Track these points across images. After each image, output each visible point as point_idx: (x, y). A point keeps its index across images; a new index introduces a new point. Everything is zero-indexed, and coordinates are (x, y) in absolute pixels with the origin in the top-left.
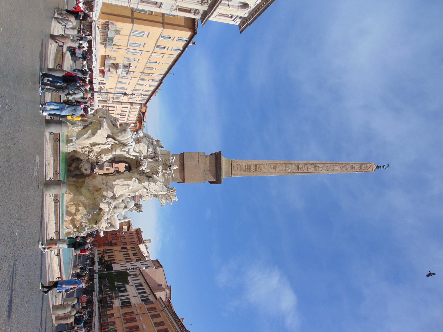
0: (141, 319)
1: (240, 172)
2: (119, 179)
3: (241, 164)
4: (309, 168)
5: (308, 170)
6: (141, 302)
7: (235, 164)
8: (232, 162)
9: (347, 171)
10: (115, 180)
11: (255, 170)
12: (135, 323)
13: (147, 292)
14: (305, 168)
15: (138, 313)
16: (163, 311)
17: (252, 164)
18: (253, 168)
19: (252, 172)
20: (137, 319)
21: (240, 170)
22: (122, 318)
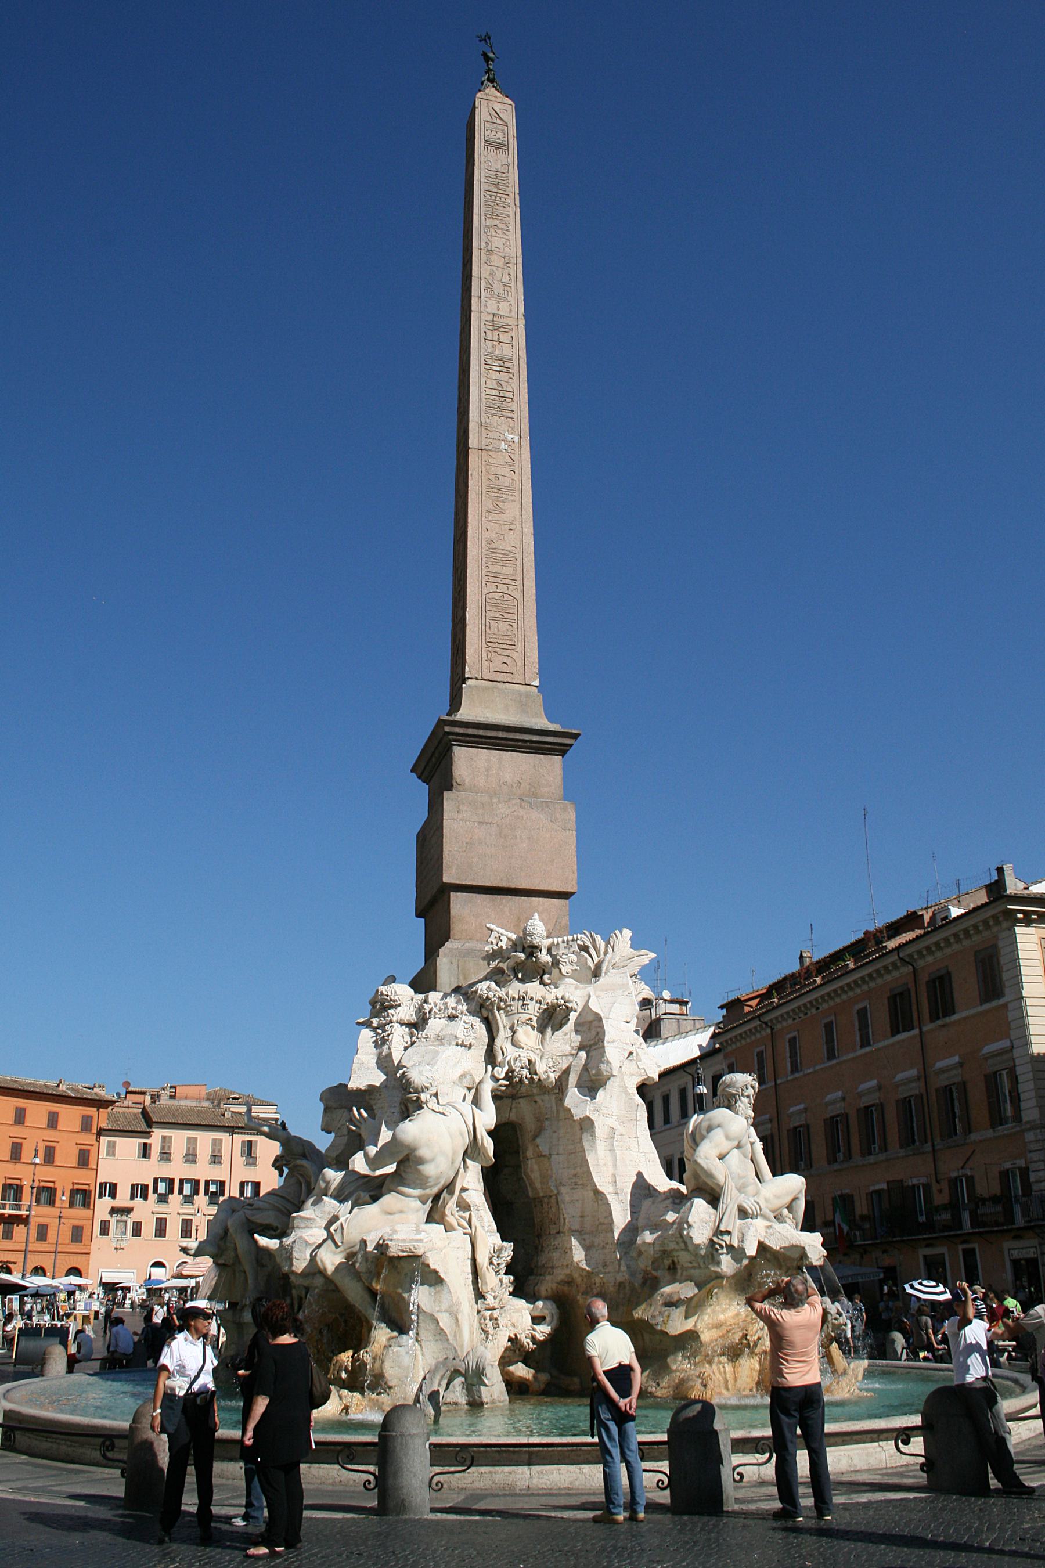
0: (802, 1106)
1: (520, 649)
3: (483, 640)
5: (510, 360)
7: (485, 664)
8: (477, 679)
9: (512, 204)
10: (597, 1193)
13: (683, 1086)
14: (498, 369)
16: (772, 1029)
17: (485, 591)
20: (797, 1124)
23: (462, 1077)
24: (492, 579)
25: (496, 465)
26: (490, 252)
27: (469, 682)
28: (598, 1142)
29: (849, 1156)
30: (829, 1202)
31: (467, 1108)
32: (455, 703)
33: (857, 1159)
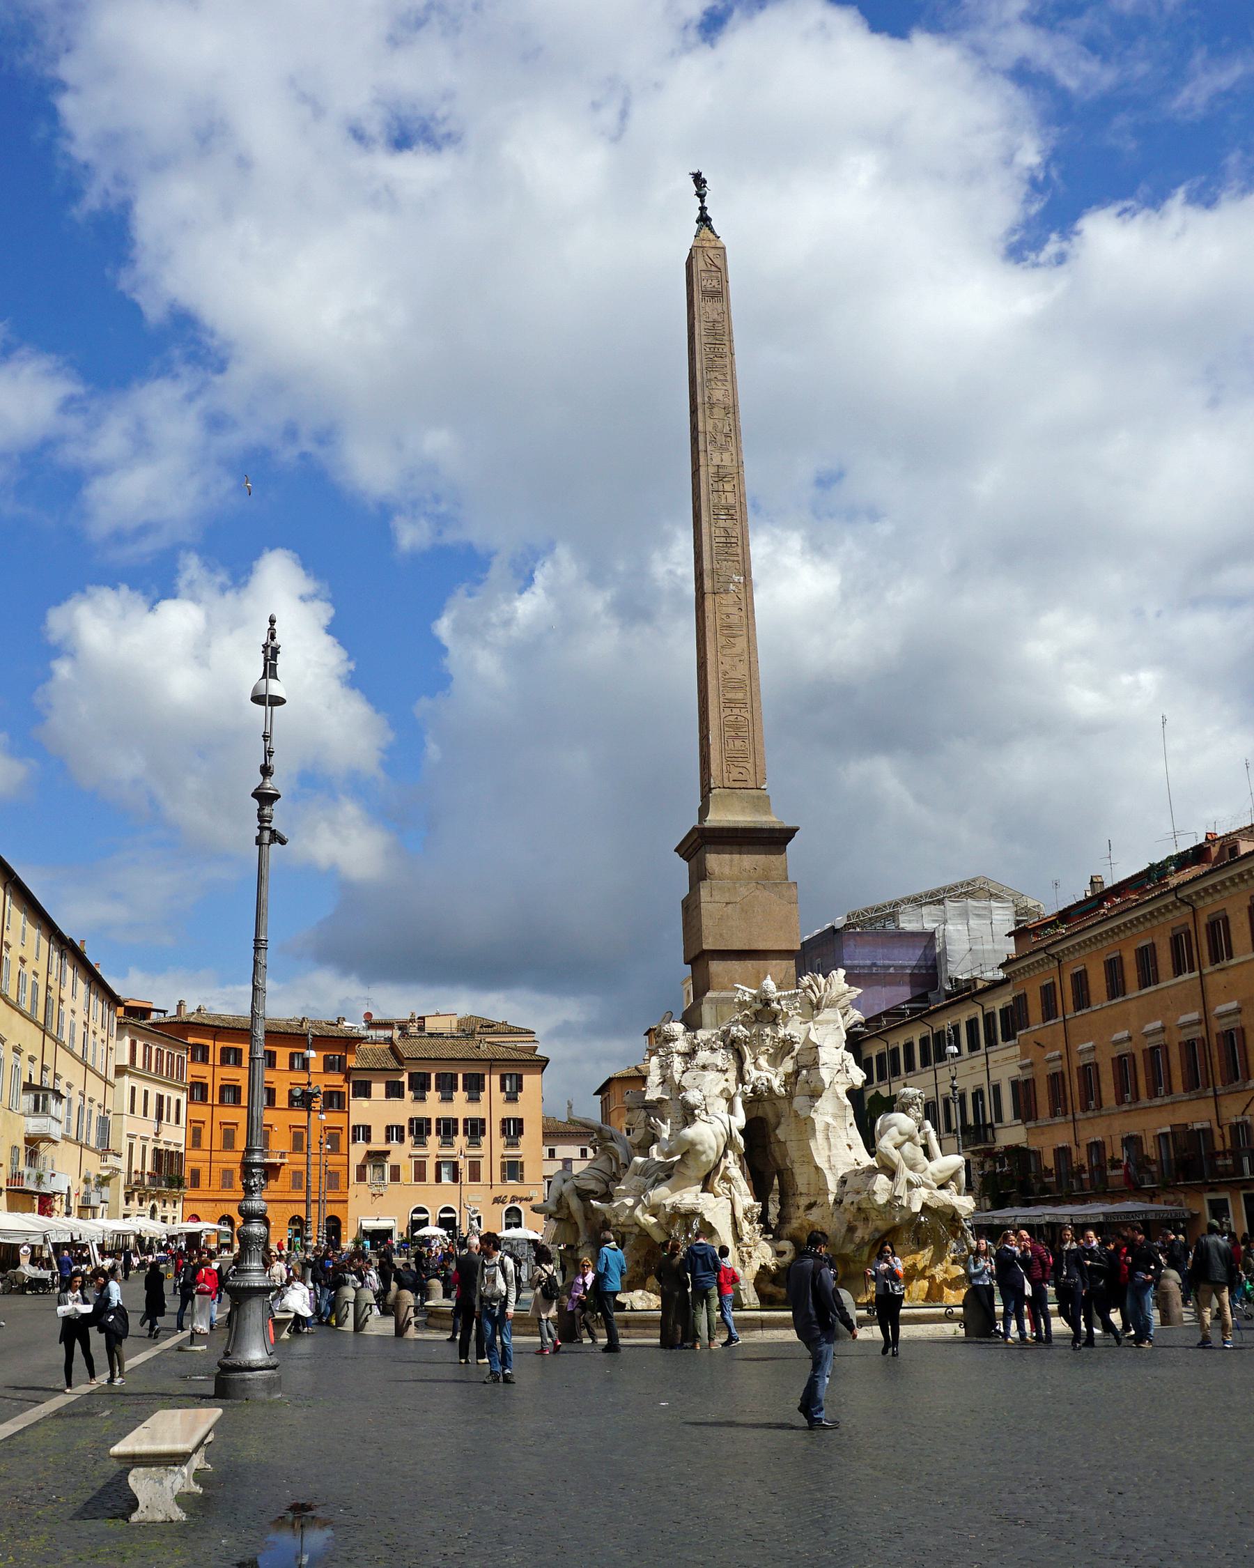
0: (1090, 1044)
2: (809, 1159)
4: (723, 501)
6: (1009, 1043)
7: (726, 775)
9: (728, 354)
11: (743, 706)
12: (1101, 1069)
13: (973, 1017)
14: (724, 517)
15: (1061, 1057)
17: (723, 716)
18: (736, 711)
19: (748, 716)
20: (1085, 1062)
21: (744, 759)
22: (1079, 1115)
23: (722, 1092)
24: (727, 705)
25: (727, 606)
26: (712, 406)
27: (714, 791)
28: (817, 1133)
29: (1137, 1098)
30: (1119, 1143)
31: (725, 1117)
32: (703, 811)
33: (1144, 1101)
